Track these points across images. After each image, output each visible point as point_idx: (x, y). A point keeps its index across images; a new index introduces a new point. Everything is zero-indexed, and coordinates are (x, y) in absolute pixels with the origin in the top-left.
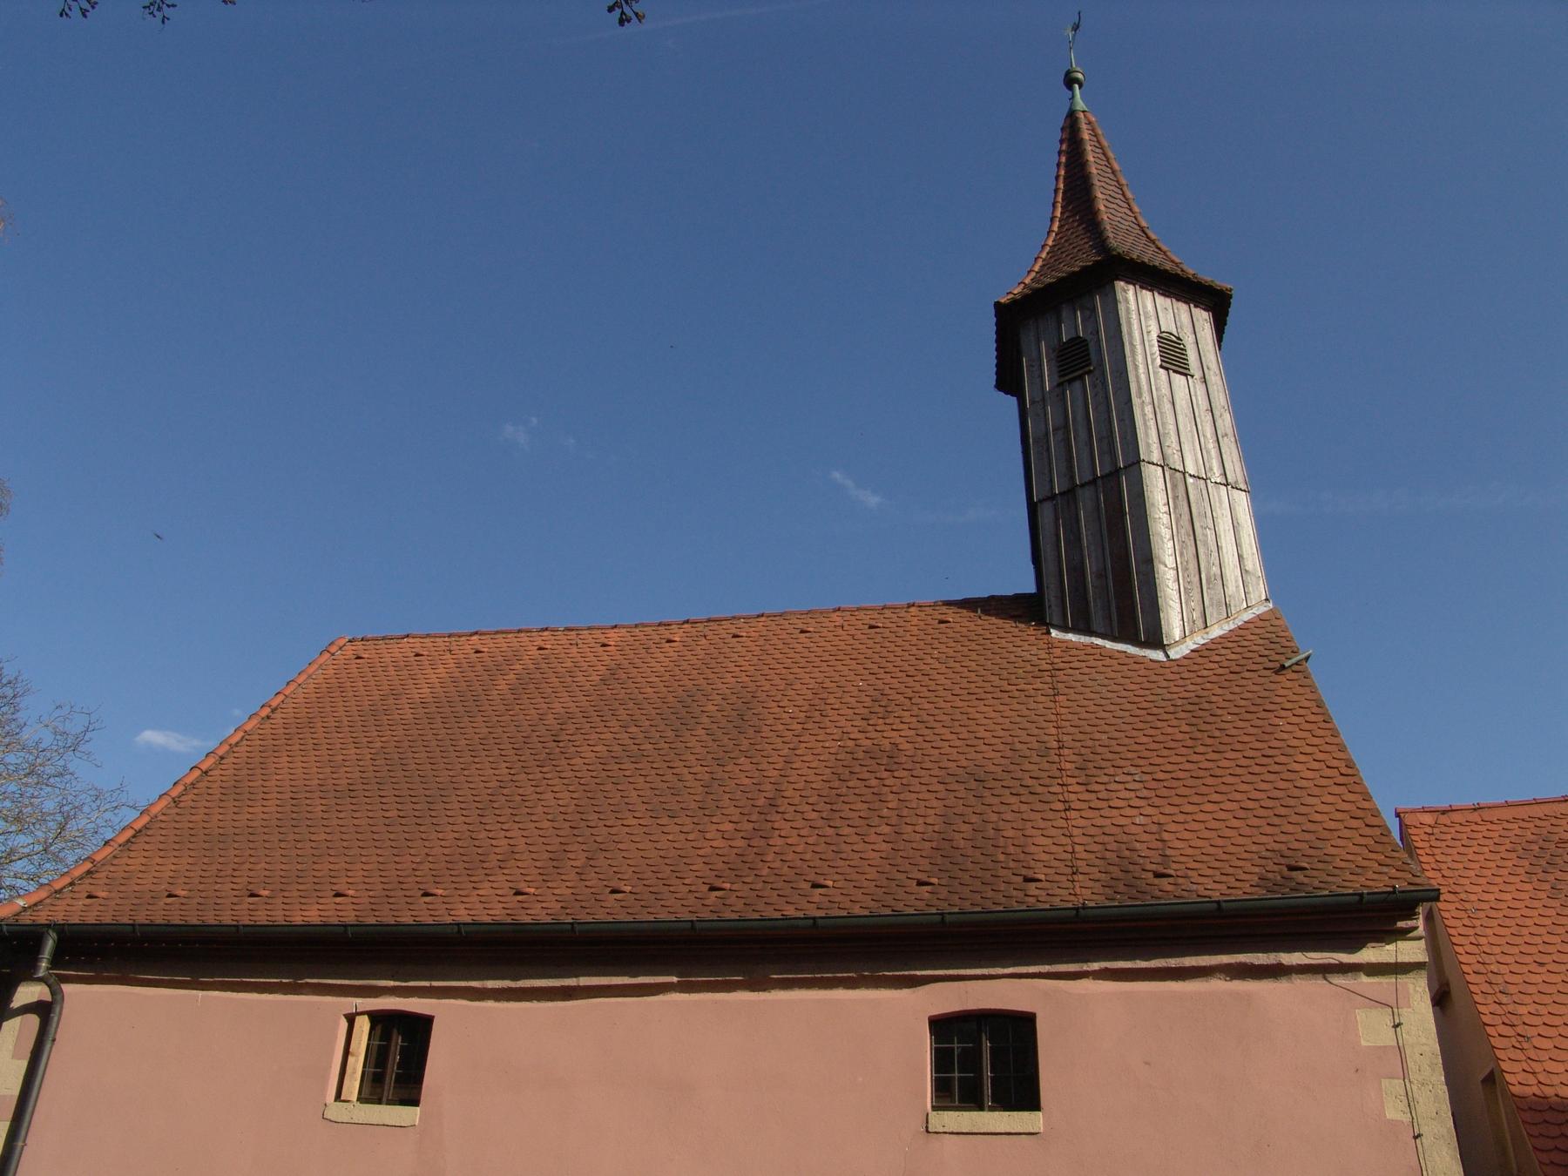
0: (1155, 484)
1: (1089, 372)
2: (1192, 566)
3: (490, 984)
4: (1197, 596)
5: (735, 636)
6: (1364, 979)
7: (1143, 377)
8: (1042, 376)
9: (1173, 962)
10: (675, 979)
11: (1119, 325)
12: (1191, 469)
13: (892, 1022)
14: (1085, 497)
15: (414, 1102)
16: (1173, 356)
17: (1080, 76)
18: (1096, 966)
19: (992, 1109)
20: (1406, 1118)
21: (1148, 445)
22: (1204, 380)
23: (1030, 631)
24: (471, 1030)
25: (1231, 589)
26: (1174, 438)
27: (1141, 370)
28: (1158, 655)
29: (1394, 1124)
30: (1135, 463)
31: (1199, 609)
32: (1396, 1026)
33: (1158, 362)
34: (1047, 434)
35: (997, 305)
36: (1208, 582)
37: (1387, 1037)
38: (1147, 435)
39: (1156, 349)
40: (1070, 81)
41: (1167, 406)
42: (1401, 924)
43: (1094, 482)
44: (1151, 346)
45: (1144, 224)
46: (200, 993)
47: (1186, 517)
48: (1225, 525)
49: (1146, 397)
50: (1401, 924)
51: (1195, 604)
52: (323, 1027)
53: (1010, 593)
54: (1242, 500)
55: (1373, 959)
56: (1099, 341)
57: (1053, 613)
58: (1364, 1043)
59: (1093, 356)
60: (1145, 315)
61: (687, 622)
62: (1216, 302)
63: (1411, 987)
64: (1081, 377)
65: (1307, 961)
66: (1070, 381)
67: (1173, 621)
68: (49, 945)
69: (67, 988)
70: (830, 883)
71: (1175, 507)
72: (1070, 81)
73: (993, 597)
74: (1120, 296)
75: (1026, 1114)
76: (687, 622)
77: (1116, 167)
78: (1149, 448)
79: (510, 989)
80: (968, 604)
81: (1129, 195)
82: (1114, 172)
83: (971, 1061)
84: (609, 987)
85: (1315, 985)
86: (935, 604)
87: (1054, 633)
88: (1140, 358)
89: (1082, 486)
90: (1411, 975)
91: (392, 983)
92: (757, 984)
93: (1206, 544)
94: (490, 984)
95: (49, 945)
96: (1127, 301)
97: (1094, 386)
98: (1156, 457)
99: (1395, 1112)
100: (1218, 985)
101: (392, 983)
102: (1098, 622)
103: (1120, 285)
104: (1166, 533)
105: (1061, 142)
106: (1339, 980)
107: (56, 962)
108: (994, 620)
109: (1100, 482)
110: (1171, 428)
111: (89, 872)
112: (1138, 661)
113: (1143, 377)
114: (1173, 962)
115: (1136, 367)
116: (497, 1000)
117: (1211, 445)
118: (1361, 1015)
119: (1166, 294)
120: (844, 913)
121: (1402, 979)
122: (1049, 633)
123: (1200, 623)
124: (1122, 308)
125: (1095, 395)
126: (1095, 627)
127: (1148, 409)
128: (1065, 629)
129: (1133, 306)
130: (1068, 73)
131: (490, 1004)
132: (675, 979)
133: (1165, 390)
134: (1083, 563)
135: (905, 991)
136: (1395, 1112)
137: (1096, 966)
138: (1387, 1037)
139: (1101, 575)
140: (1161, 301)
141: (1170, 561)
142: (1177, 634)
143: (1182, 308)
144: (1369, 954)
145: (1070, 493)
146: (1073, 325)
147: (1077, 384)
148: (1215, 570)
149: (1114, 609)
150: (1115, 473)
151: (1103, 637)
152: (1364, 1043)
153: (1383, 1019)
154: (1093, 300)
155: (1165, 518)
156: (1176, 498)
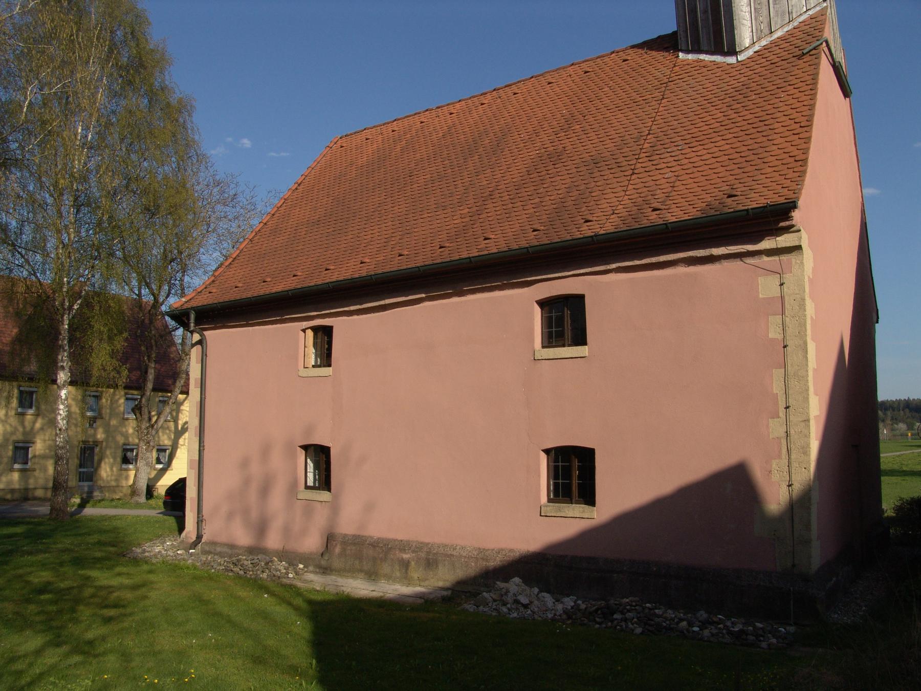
3: (352, 308)
4: (765, 12)
5: (625, 61)
6: (765, 258)
9: (654, 260)
10: (424, 295)
15: (330, 366)
18: (614, 266)
19: (569, 346)
20: (780, 337)
24: (349, 328)
28: (732, 60)
29: (773, 340)
31: (766, 21)
32: (782, 284)
37: (775, 291)
42: (782, 224)
46: (250, 328)
50: (782, 224)
51: (763, 18)
52: (294, 337)
55: (768, 247)
57: (682, 44)
58: (761, 296)
61: (613, 52)
63: (794, 261)
65: (727, 252)
67: (746, 34)
68: (192, 316)
69: (206, 333)
70: (739, 193)
73: (659, 37)
75: (579, 347)
76: (613, 52)
80: (633, 47)
83: (560, 321)
84: (398, 303)
85: (736, 264)
86: (626, 49)
87: (681, 55)
90: (793, 254)
91: (315, 313)
92: (461, 294)
94: (352, 308)
95: (192, 316)
100: (681, 270)
101: (315, 313)
106: (750, 260)
107: (198, 322)
108: (654, 53)
111: (213, 281)
112: (718, 65)
114: (654, 260)
118: (761, 280)
121: (784, 258)
123: (767, 31)
128: (687, 52)
131: (355, 317)
132: (424, 295)
134: (696, 5)
135: (526, 290)
136: (774, 333)
137: (614, 266)
138: (775, 291)
142: (747, 43)
144: (767, 244)
151: (707, 53)
153: (776, 280)
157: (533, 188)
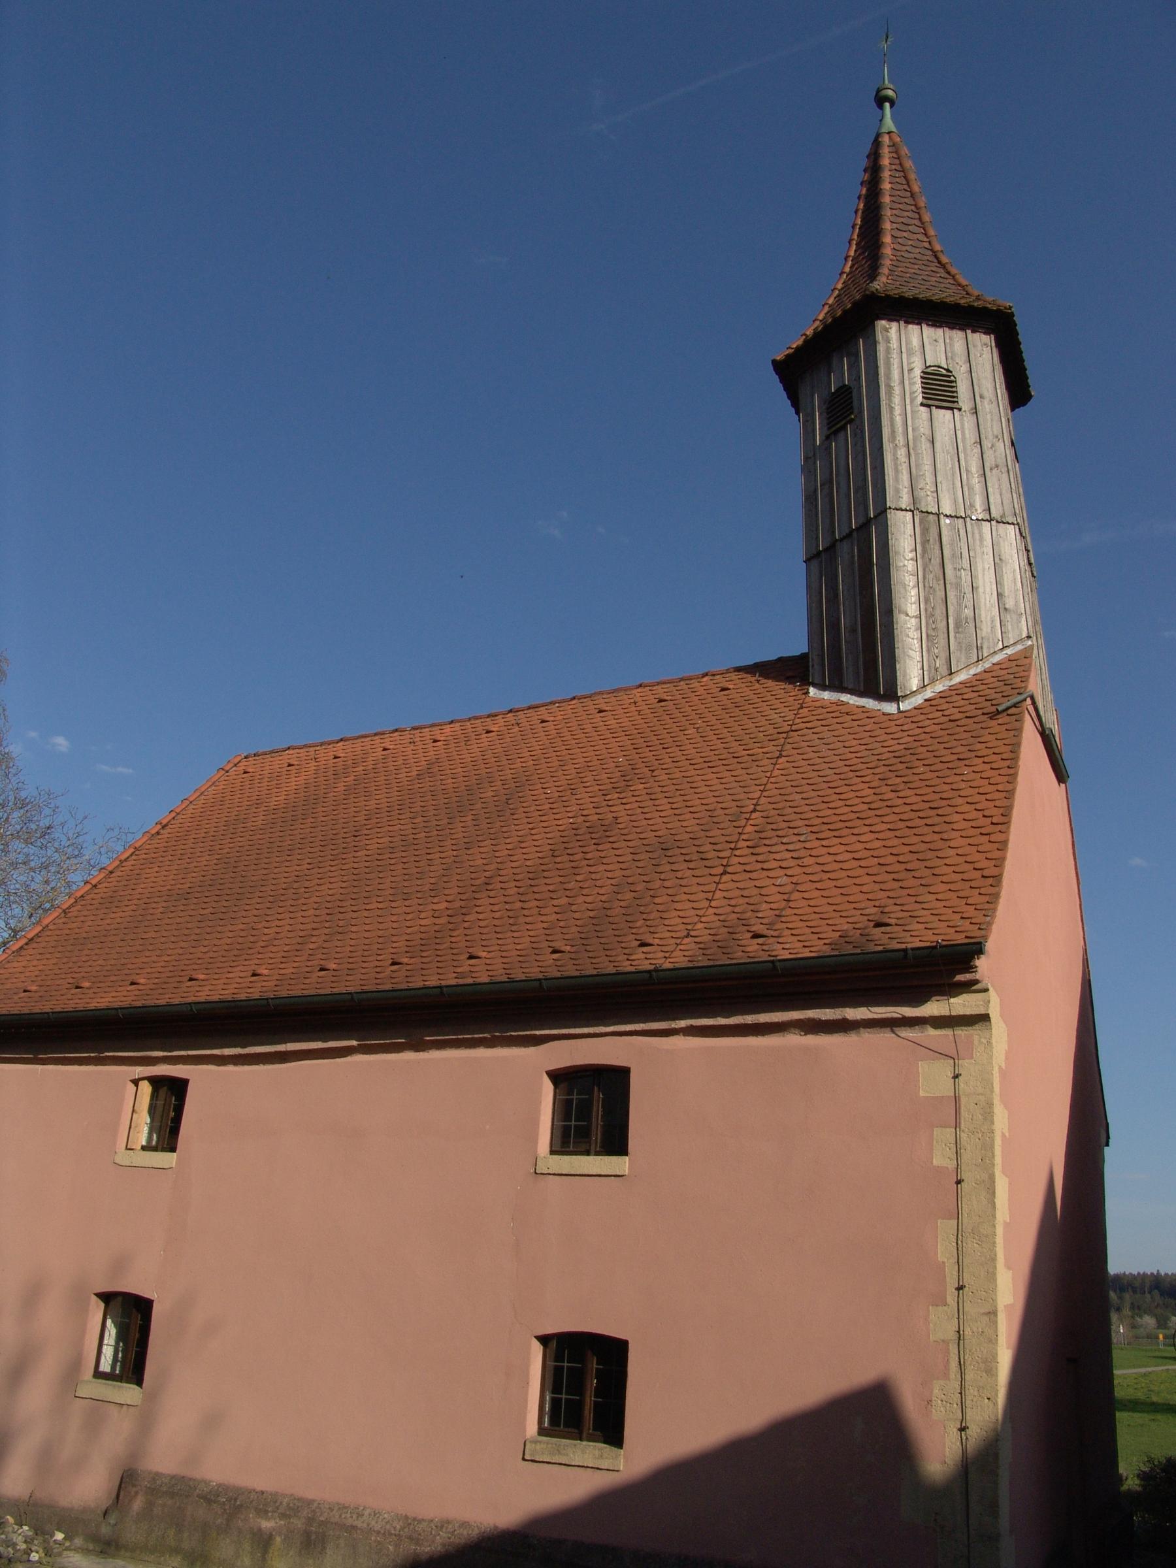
0: (903, 535)
1: (851, 421)
2: (939, 611)
3: (227, 1052)
4: (942, 641)
5: (723, 689)
6: (931, 1032)
7: (898, 420)
8: (814, 430)
9: (749, 1019)
10: (354, 1043)
11: (877, 367)
12: (947, 509)
13: (519, 1078)
14: (844, 549)
15: (173, 1149)
16: (939, 389)
17: (890, 93)
18: (682, 1023)
19: (597, 1154)
20: (951, 1165)
21: (897, 491)
22: (975, 411)
23: (793, 690)
24: (219, 1087)
25: (985, 629)
26: (929, 478)
27: (898, 411)
28: (890, 708)
29: (939, 1170)
30: (883, 511)
32: (956, 1077)
33: (920, 399)
34: (816, 490)
35: (774, 362)
36: (958, 625)
37: (945, 1088)
38: (897, 479)
39: (918, 387)
40: (880, 100)
41: (925, 446)
42: (960, 978)
43: (849, 535)
44: (912, 384)
45: (938, 247)
46: (40, 1067)
47: (936, 561)
48: (984, 565)
49: (900, 439)
50: (960, 978)
51: (940, 650)
52: (117, 1091)
53: (798, 654)
54: (1011, 531)
56: (860, 387)
58: (922, 1094)
59: (855, 404)
60: (907, 351)
61: (707, 674)
62: (1000, 325)
63: (976, 1038)
64: (844, 428)
66: (836, 433)
67: (912, 671)
70: (893, 921)
71: (924, 551)
72: (880, 100)
73: (780, 659)
74: (880, 337)
75: (614, 1158)
76: (707, 674)
77: (916, 189)
78: (898, 491)
79: (240, 1056)
80: (738, 669)
81: (927, 217)
82: (913, 195)
83: (585, 1111)
84: (310, 1051)
86: (728, 671)
88: (897, 400)
89: (841, 540)
90: (977, 1027)
91: (161, 1054)
92: (419, 1046)
93: (958, 586)
94: (227, 1052)
96: (888, 341)
97: (854, 435)
98: (905, 501)
99: (942, 1158)
100: (794, 1040)
101: (161, 1054)
102: (849, 682)
103: (883, 323)
104: (910, 581)
105: (865, 171)
106: (906, 1033)
109: (855, 534)
110: (927, 469)
113: (898, 420)
114: (749, 1019)
115: (891, 409)
116: (235, 1064)
117: (976, 481)
118: (923, 1067)
119: (936, 324)
120: (880, 948)
121: (962, 1032)
122: (808, 693)
123: (944, 670)
124: (881, 349)
125: (855, 445)
126: (845, 685)
127: (902, 453)
128: (823, 687)
129: (894, 344)
130: (878, 91)
131: (231, 1068)
132: (354, 1043)
133: (924, 428)
134: (839, 619)
135: (532, 1049)
136: (942, 1158)
137: (682, 1023)
138: (945, 1088)
139: (853, 631)
140: (928, 331)
141: (912, 609)
142: (914, 684)
143: (957, 335)
144: (934, 1008)
145: (831, 548)
146: (841, 373)
147: (841, 435)
148: (968, 612)
149: (861, 663)
150: (865, 525)
152: (922, 1094)
153: (944, 1069)
154: (857, 344)
155: (910, 566)
156: (925, 542)
157: (555, 917)
